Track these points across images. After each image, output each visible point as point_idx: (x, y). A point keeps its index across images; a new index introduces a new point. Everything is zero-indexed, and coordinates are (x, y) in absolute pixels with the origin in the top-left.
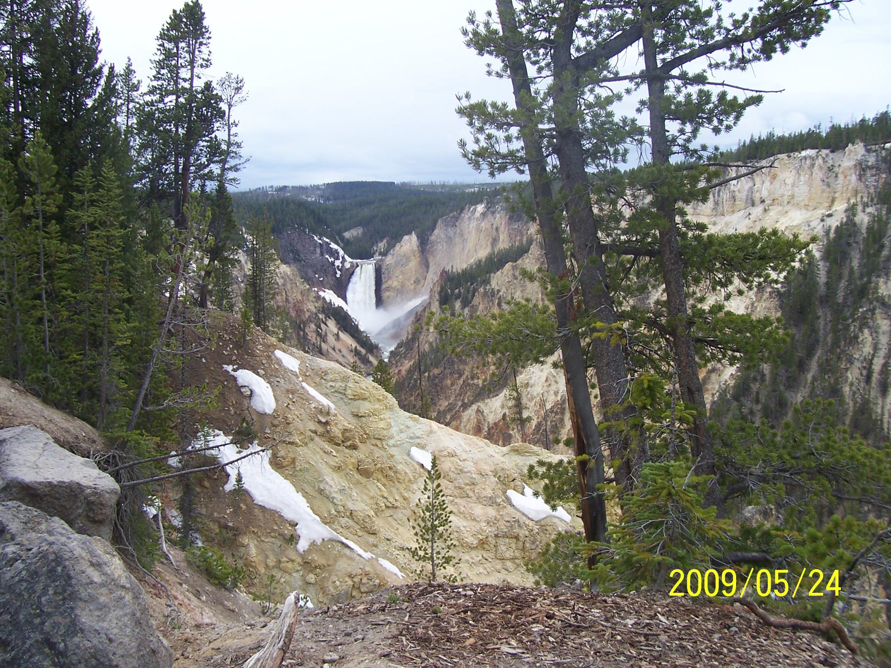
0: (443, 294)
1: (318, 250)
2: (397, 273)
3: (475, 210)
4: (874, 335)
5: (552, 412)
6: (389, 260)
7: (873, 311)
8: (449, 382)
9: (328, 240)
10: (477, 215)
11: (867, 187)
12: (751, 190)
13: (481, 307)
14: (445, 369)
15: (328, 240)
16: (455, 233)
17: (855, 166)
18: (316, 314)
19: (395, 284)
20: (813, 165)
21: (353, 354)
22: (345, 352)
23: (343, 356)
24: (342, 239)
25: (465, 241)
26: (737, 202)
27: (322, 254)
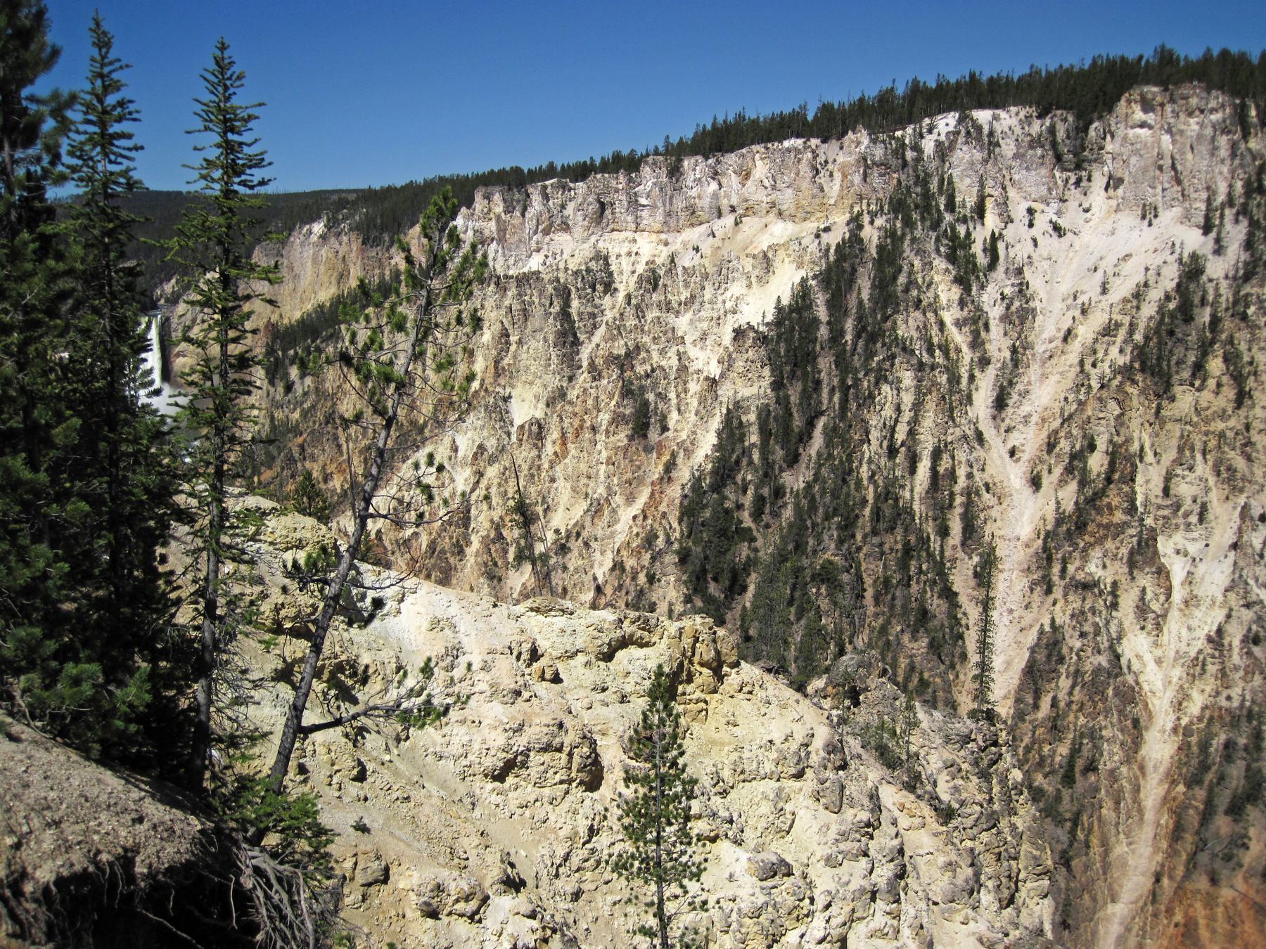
10: (314, 238)
12: (715, 196)
25: (296, 277)
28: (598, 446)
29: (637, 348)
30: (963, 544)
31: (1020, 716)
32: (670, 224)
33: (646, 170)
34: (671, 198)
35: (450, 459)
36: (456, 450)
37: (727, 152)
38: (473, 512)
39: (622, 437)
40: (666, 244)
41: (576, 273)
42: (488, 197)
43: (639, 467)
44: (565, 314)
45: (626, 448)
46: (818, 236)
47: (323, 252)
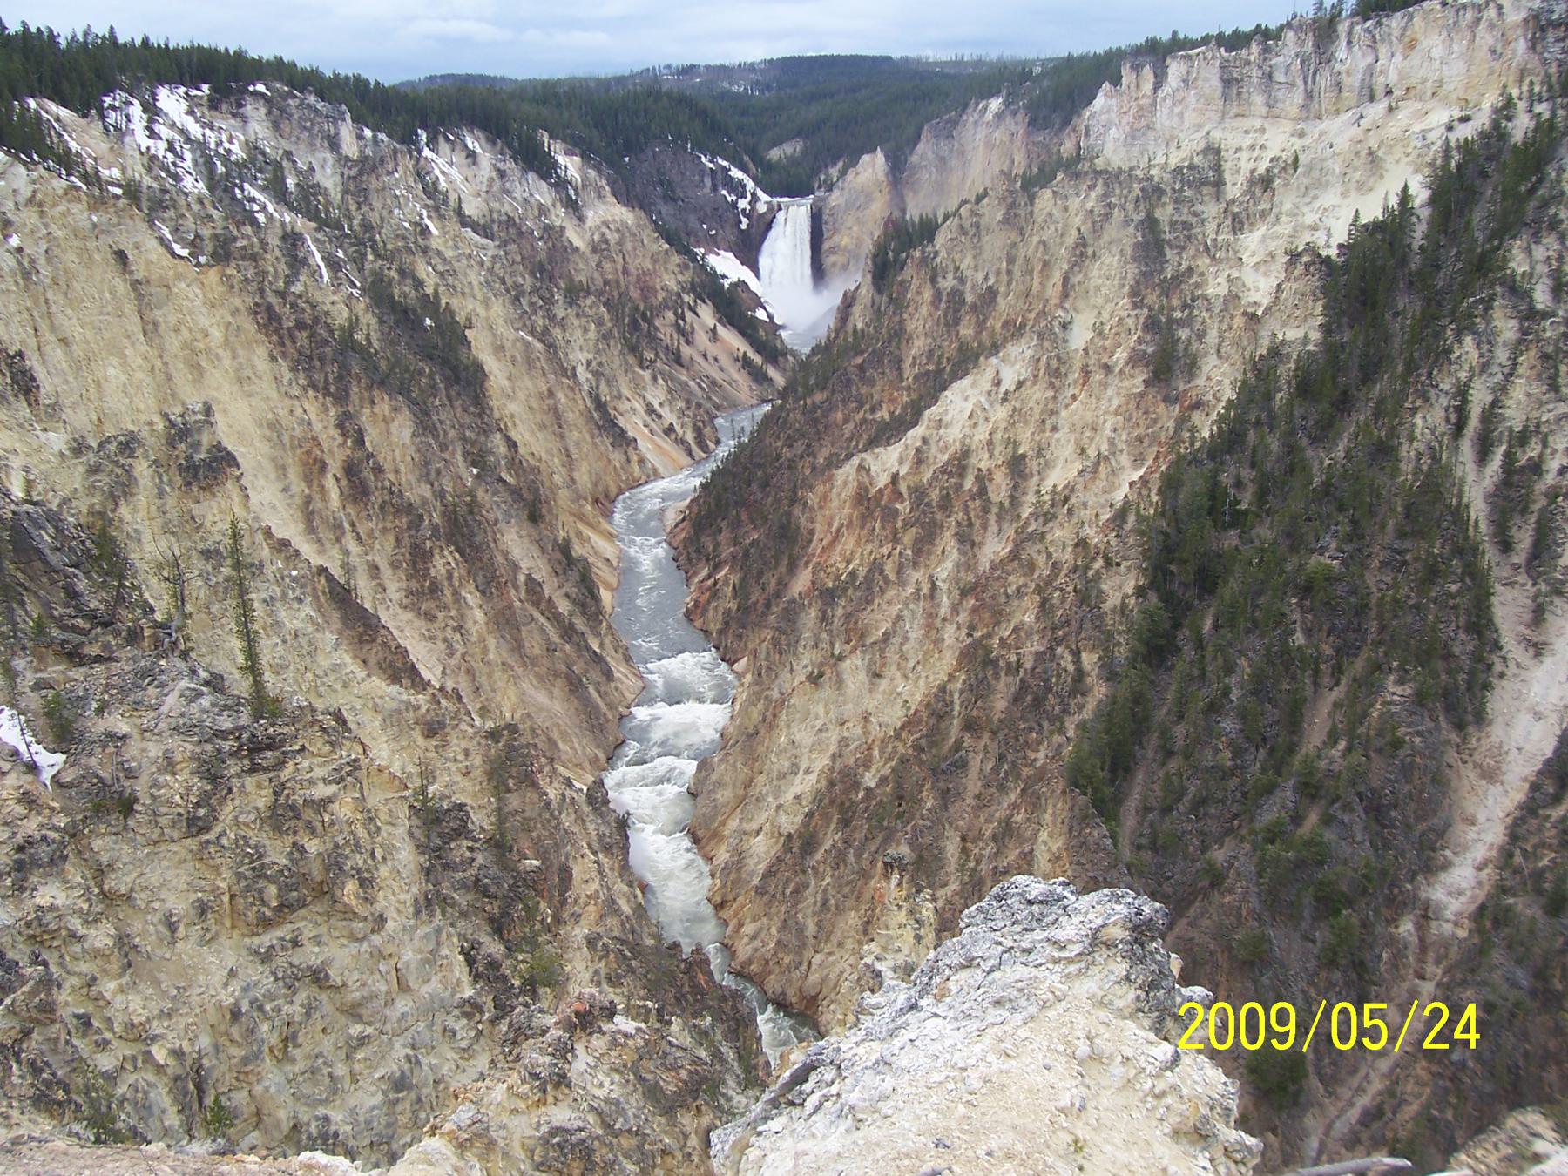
0: (878, 260)
1: (708, 182)
2: (850, 221)
3: (985, 108)
4: (1485, 347)
5: (944, 472)
6: (835, 198)
7: (1488, 303)
8: (840, 416)
9: (725, 163)
10: (989, 116)
11: (1545, 62)
12: (1370, 71)
13: (915, 284)
14: (833, 392)
15: (725, 163)
16: (951, 151)
17: (1526, 21)
18: (679, 295)
19: (846, 241)
20: (1478, 21)
21: (739, 365)
22: (725, 361)
23: (721, 369)
24: (759, 161)
26: (1345, 94)
27: (715, 188)
28: (1110, 392)
29: (1190, 270)
30: (1529, 562)
31: (1530, 809)
32: (1310, 109)
33: (1290, 36)
34: (1315, 74)
35: (989, 393)
36: (998, 384)
37: (1395, 10)
38: (973, 461)
39: (1137, 382)
40: (1302, 135)
41: (1178, 170)
42: (1137, 68)
43: (1155, 421)
44: (1150, 224)
45: (1142, 395)
46: (1450, 128)
47: (997, 134)
